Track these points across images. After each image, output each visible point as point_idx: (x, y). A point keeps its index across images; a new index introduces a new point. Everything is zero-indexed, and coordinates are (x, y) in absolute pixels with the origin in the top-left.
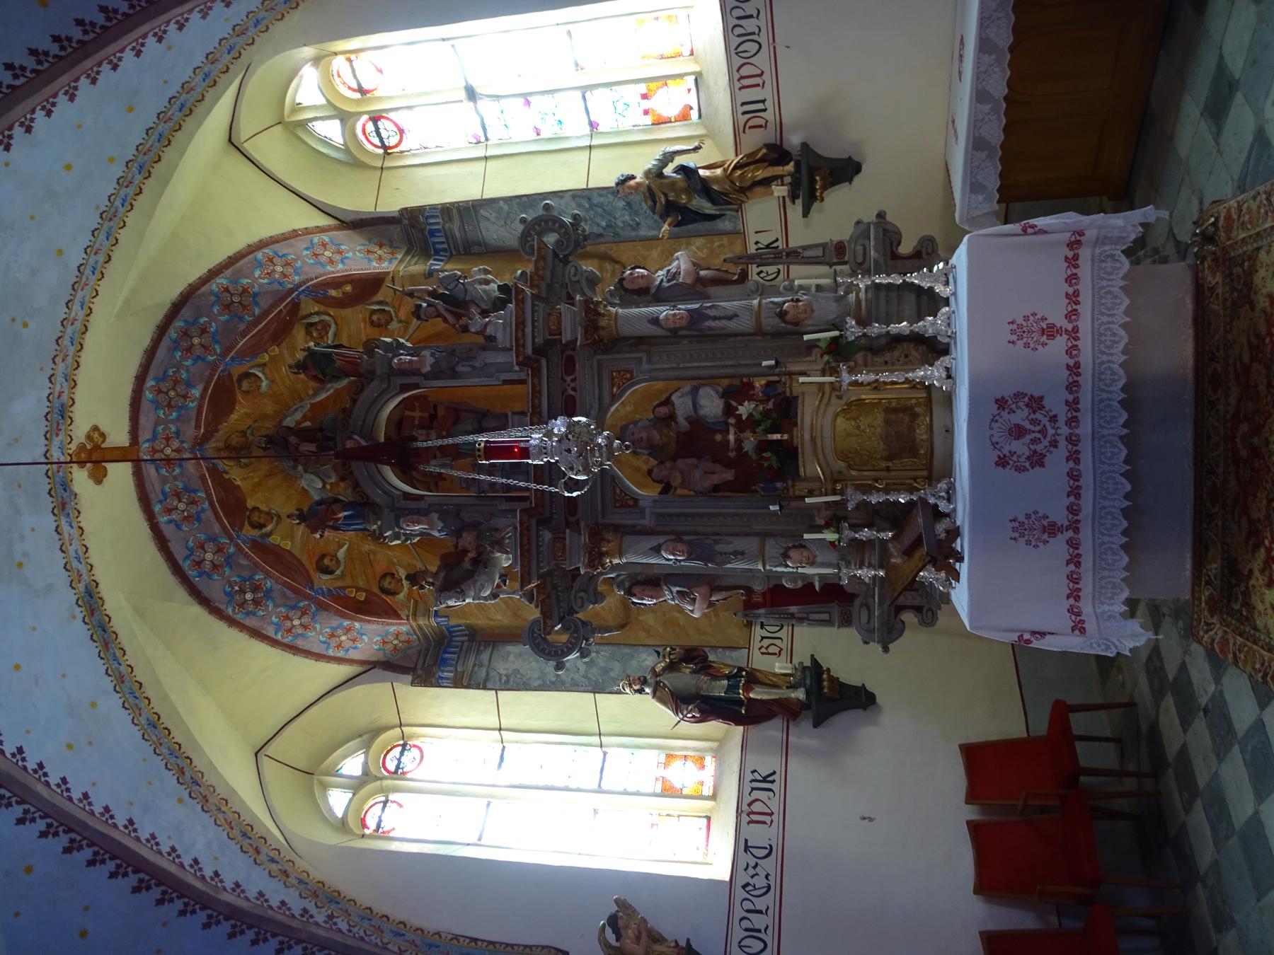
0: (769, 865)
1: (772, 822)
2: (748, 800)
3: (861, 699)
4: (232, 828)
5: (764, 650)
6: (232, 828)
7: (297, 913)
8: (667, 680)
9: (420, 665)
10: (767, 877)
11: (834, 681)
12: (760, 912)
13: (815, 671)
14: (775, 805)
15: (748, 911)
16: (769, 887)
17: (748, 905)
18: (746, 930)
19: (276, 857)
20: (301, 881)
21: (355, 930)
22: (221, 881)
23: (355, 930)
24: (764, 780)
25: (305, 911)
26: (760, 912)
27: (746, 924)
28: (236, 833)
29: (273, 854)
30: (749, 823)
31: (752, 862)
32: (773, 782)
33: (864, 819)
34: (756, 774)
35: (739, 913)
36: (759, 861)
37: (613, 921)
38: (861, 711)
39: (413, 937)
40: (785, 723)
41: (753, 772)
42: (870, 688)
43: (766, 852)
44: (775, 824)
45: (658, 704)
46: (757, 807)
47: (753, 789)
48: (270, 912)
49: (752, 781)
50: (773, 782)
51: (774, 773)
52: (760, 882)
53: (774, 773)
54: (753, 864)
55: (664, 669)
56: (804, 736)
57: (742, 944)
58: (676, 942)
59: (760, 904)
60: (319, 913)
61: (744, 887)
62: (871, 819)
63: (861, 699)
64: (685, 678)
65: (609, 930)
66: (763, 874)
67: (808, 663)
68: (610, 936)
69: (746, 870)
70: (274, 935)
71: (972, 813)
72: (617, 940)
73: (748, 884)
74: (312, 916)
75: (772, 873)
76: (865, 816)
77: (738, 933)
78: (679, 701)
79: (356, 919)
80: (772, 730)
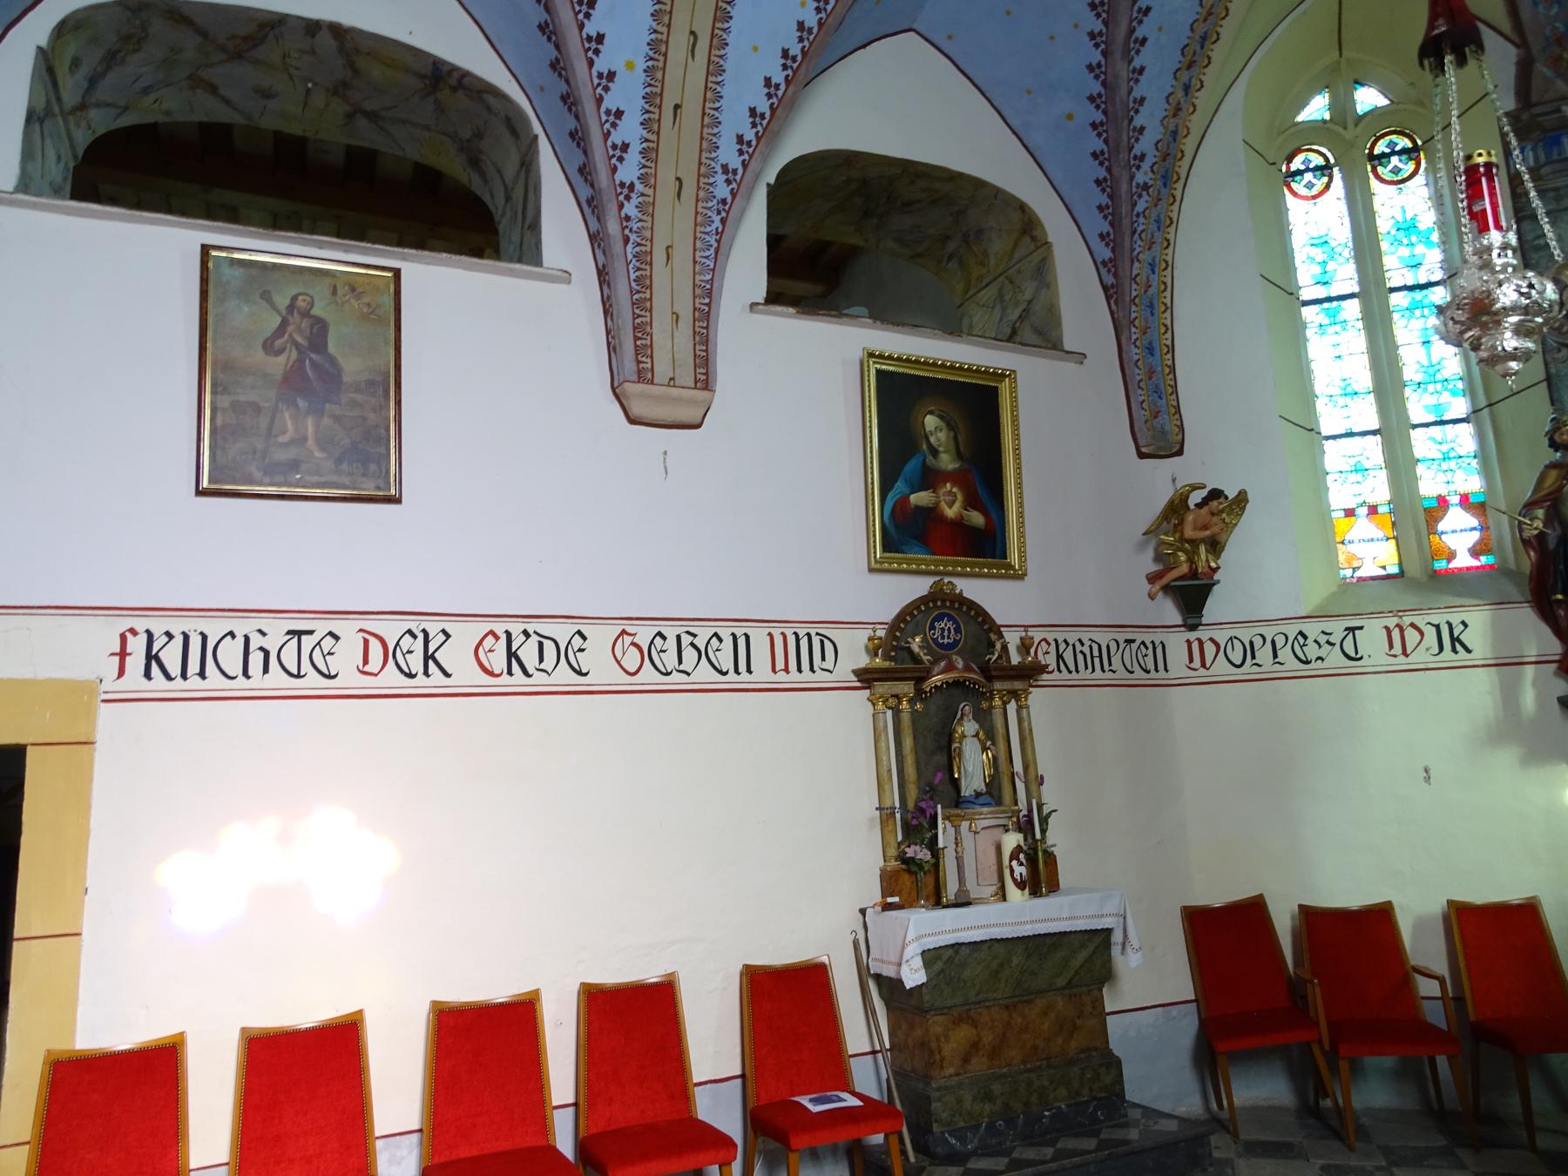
0: (1335, 659)
1: (1395, 656)
2: (1420, 621)
4: (1205, 20)
6: (1205, 20)
7: (1137, 151)
9: (1536, 110)
10: (1319, 658)
12: (1275, 656)
14: (1419, 657)
15: (1273, 642)
16: (1307, 662)
17: (1280, 641)
18: (1251, 643)
19: (1192, 90)
20: (1175, 133)
21: (1142, 220)
22: (1138, 52)
23: (1142, 220)
24: (1455, 640)
25: (1142, 157)
26: (1275, 656)
27: (1258, 642)
28: (1201, 28)
29: (1195, 83)
30: (1387, 628)
31: (1336, 639)
32: (1454, 650)
33: (1426, 771)
34: (1462, 627)
35: (1269, 632)
36: (1338, 646)
37: (1216, 494)
39: (1155, 284)
40: (1557, 658)
41: (1465, 624)
43: (1352, 654)
45: (1535, 479)
46: (1412, 636)
47: (1438, 627)
48: (1126, 122)
49: (1450, 625)
51: (1469, 651)
52: (1312, 651)
53: (1469, 651)
54: (1332, 640)
57: (1235, 641)
58: (1219, 568)
59: (1285, 654)
60: (1146, 173)
61: (1301, 633)
62: (1428, 779)
65: (1204, 493)
66: (1322, 653)
68: (1196, 497)
69: (1323, 632)
70: (1106, 141)
72: (1196, 505)
73: (1305, 637)
74: (1138, 168)
75: (1325, 664)
76: (1432, 773)
77: (1245, 635)
79: (1154, 216)
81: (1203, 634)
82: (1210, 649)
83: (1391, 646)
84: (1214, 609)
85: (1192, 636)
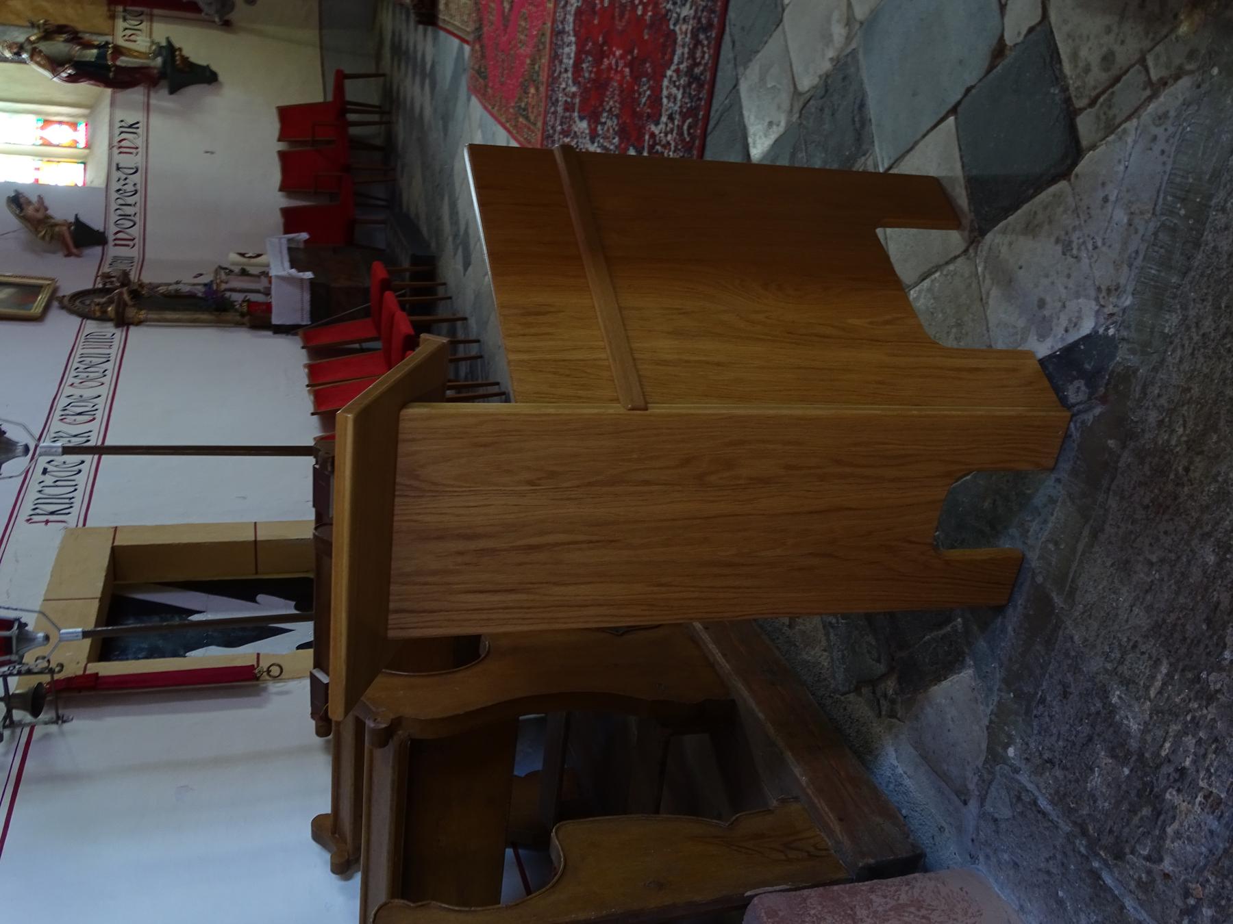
0: (136, 178)
3: (207, 77)
5: (126, 38)
8: (43, 46)
11: (185, 60)
12: (130, 205)
13: (170, 50)
14: (139, 142)
18: (120, 215)
24: (130, 126)
26: (130, 205)
27: (119, 212)
32: (138, 128)
35: (114, 206)
38: (205, 85)
42: (214, 68)
44: (140, 154)
47: (122, 132)
50: (138, 128)
51: (138, 123)
52: (129, 188)
53: (138, 123)
55: (39, 39)
56: (161, 98)
59: (130, 200)
62: (212, 153)
63: (207, 77)
64: (59, 46)
67: (164, 43)
71: (282, 146)
77: (114, 217)
78: (54, 64)
80: (136, 95)
81: (111, 237)
82: (120, 235)
83: (131, 153)
84: (96, 224)
85: (111, 243)
